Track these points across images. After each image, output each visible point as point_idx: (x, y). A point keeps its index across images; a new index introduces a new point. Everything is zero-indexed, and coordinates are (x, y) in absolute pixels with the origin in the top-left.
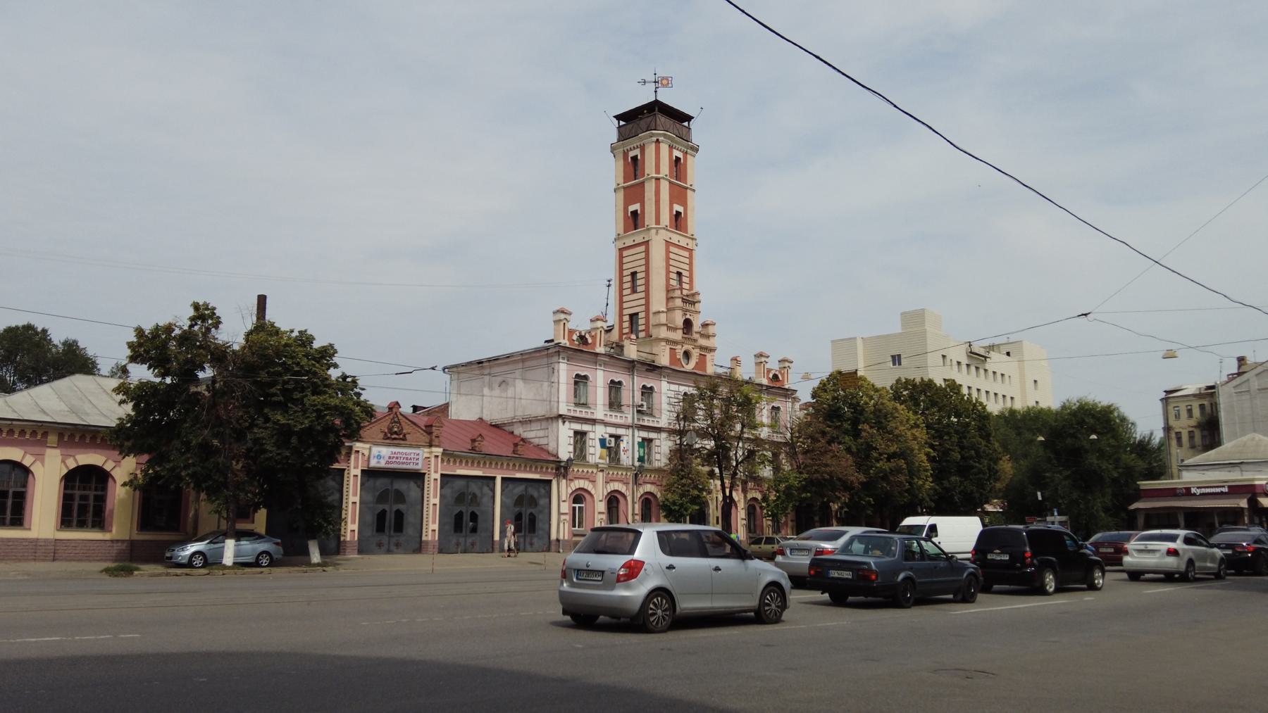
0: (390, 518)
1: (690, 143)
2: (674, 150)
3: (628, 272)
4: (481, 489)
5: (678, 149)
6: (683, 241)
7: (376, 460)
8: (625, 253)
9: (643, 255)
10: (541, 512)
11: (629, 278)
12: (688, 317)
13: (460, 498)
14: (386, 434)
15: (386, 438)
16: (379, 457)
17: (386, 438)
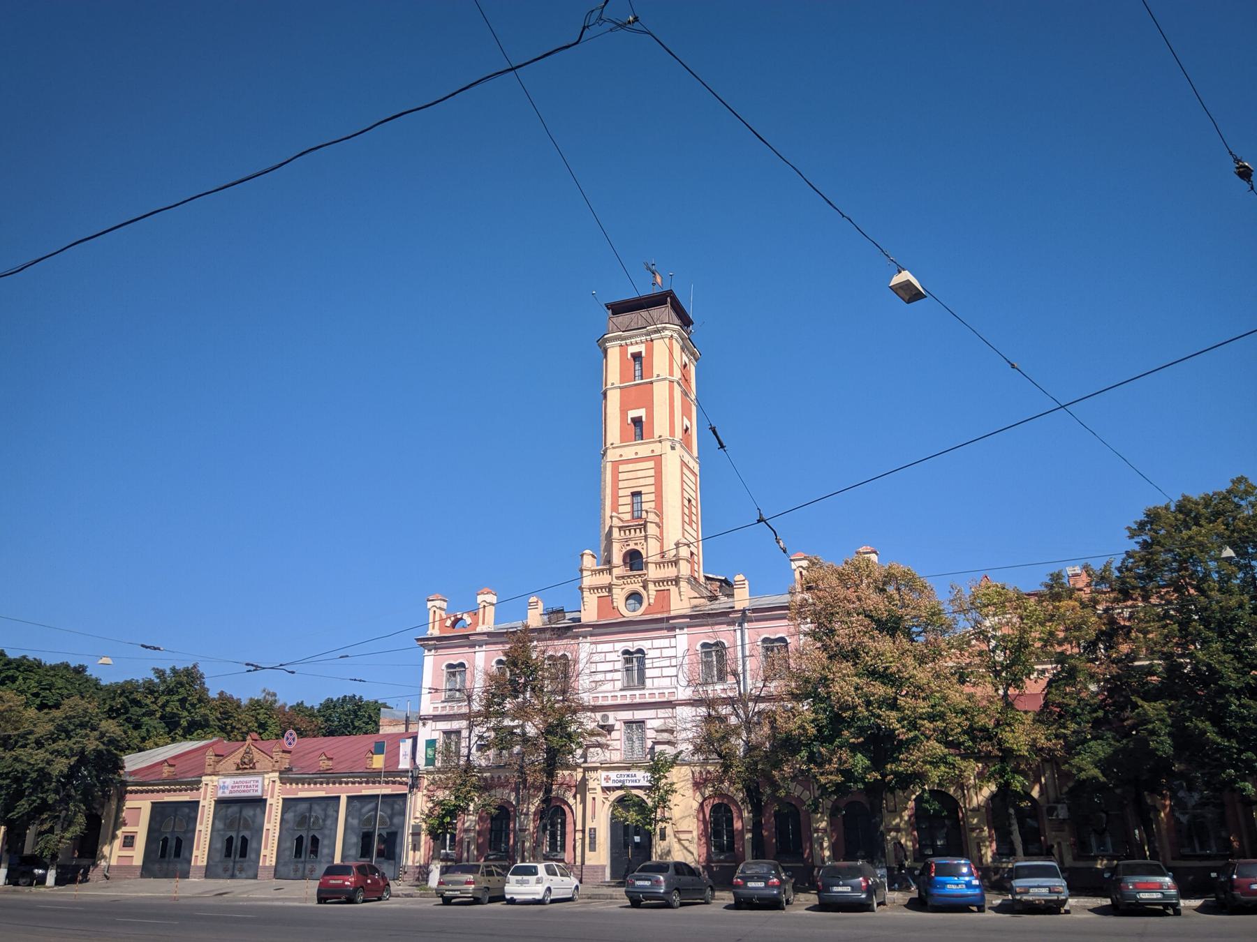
0: (237, 843)
4: (325, 810)
5: (637, 343)
7: (222, 790)
10: (324, 836)
12: (632, 546)
13: (303, 821)
15: (238, 769)
16: (224, 787)
17: (238, 769)
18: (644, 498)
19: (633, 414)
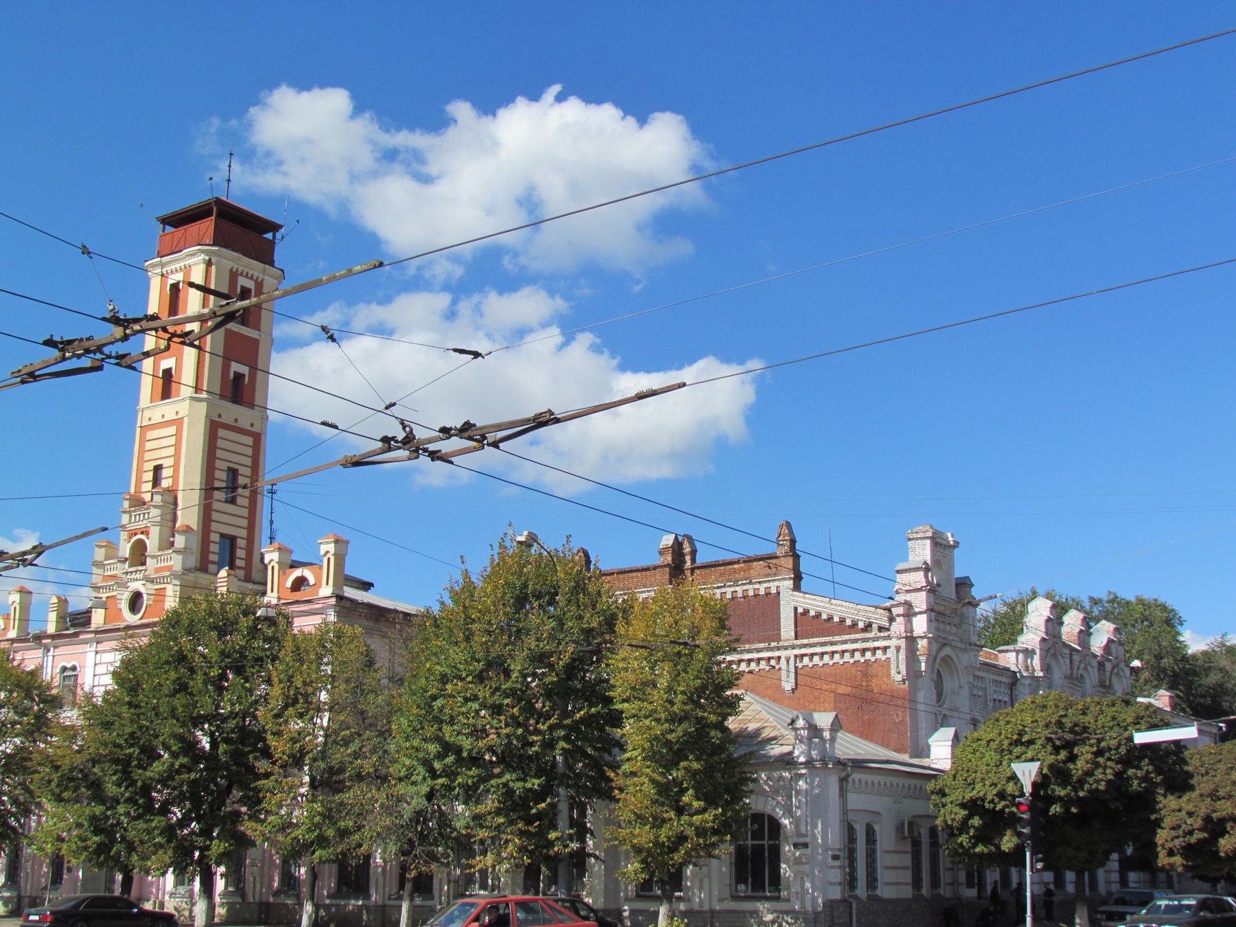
2: (240, 278)
3: (150, 466)
5: (247, 276)
6: (244, 424)
8: (151, 435)
9: (172, 441)
11: (149, 476)
19: (236, 367)
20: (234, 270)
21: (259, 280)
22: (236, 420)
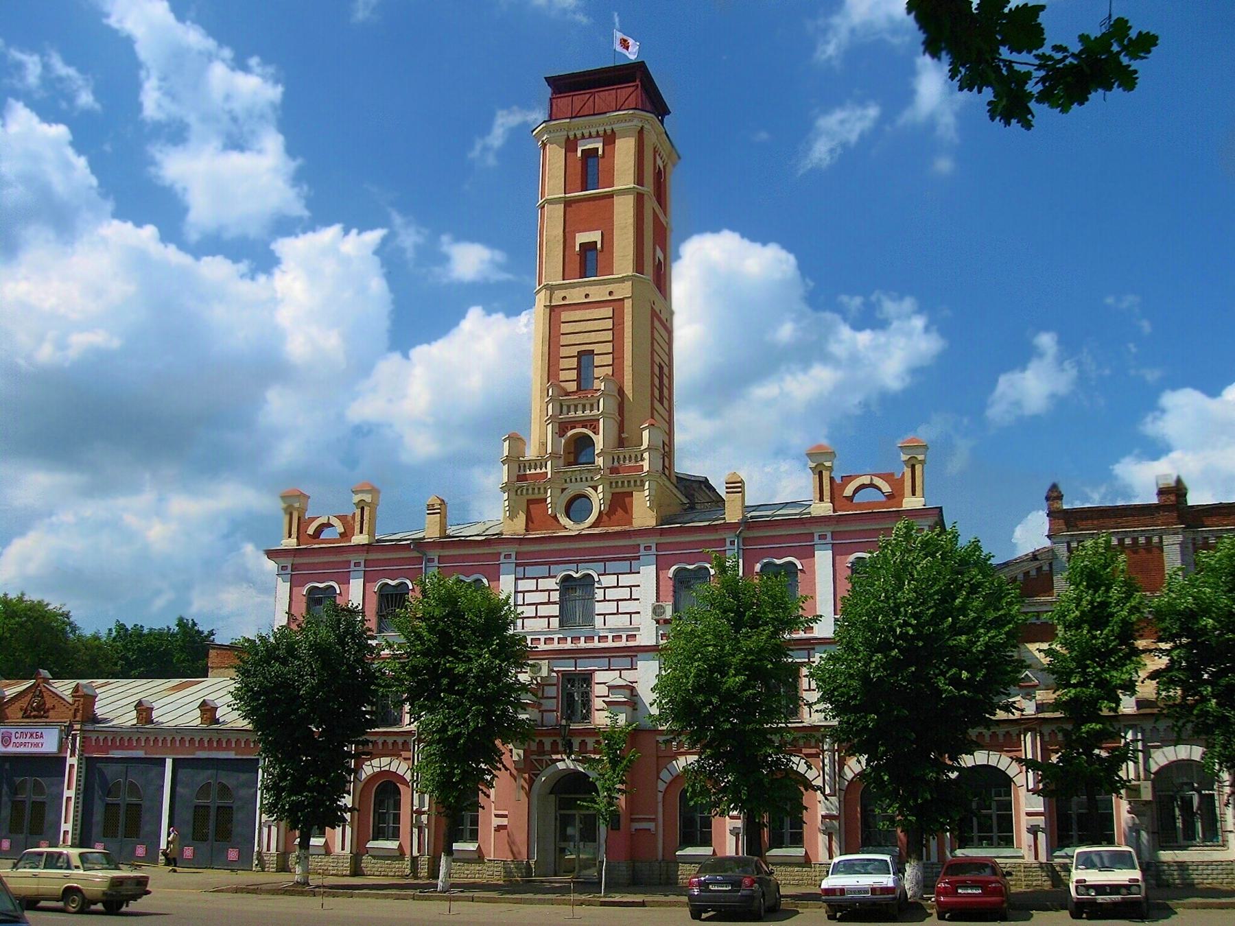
1: (608, 115)
5: (590, 136)
14: (26, 711)
18: (597, 360)
19: (582, 238)
20: (572, 137)
21: (609, 132)
22: (587, 296)
